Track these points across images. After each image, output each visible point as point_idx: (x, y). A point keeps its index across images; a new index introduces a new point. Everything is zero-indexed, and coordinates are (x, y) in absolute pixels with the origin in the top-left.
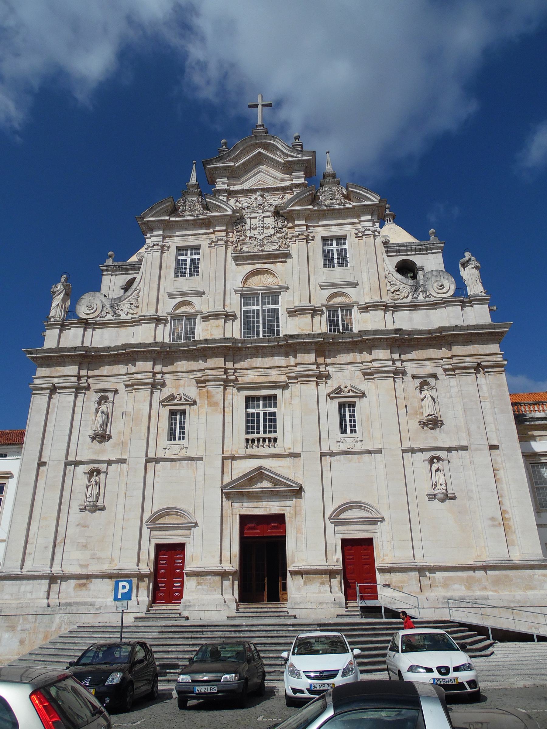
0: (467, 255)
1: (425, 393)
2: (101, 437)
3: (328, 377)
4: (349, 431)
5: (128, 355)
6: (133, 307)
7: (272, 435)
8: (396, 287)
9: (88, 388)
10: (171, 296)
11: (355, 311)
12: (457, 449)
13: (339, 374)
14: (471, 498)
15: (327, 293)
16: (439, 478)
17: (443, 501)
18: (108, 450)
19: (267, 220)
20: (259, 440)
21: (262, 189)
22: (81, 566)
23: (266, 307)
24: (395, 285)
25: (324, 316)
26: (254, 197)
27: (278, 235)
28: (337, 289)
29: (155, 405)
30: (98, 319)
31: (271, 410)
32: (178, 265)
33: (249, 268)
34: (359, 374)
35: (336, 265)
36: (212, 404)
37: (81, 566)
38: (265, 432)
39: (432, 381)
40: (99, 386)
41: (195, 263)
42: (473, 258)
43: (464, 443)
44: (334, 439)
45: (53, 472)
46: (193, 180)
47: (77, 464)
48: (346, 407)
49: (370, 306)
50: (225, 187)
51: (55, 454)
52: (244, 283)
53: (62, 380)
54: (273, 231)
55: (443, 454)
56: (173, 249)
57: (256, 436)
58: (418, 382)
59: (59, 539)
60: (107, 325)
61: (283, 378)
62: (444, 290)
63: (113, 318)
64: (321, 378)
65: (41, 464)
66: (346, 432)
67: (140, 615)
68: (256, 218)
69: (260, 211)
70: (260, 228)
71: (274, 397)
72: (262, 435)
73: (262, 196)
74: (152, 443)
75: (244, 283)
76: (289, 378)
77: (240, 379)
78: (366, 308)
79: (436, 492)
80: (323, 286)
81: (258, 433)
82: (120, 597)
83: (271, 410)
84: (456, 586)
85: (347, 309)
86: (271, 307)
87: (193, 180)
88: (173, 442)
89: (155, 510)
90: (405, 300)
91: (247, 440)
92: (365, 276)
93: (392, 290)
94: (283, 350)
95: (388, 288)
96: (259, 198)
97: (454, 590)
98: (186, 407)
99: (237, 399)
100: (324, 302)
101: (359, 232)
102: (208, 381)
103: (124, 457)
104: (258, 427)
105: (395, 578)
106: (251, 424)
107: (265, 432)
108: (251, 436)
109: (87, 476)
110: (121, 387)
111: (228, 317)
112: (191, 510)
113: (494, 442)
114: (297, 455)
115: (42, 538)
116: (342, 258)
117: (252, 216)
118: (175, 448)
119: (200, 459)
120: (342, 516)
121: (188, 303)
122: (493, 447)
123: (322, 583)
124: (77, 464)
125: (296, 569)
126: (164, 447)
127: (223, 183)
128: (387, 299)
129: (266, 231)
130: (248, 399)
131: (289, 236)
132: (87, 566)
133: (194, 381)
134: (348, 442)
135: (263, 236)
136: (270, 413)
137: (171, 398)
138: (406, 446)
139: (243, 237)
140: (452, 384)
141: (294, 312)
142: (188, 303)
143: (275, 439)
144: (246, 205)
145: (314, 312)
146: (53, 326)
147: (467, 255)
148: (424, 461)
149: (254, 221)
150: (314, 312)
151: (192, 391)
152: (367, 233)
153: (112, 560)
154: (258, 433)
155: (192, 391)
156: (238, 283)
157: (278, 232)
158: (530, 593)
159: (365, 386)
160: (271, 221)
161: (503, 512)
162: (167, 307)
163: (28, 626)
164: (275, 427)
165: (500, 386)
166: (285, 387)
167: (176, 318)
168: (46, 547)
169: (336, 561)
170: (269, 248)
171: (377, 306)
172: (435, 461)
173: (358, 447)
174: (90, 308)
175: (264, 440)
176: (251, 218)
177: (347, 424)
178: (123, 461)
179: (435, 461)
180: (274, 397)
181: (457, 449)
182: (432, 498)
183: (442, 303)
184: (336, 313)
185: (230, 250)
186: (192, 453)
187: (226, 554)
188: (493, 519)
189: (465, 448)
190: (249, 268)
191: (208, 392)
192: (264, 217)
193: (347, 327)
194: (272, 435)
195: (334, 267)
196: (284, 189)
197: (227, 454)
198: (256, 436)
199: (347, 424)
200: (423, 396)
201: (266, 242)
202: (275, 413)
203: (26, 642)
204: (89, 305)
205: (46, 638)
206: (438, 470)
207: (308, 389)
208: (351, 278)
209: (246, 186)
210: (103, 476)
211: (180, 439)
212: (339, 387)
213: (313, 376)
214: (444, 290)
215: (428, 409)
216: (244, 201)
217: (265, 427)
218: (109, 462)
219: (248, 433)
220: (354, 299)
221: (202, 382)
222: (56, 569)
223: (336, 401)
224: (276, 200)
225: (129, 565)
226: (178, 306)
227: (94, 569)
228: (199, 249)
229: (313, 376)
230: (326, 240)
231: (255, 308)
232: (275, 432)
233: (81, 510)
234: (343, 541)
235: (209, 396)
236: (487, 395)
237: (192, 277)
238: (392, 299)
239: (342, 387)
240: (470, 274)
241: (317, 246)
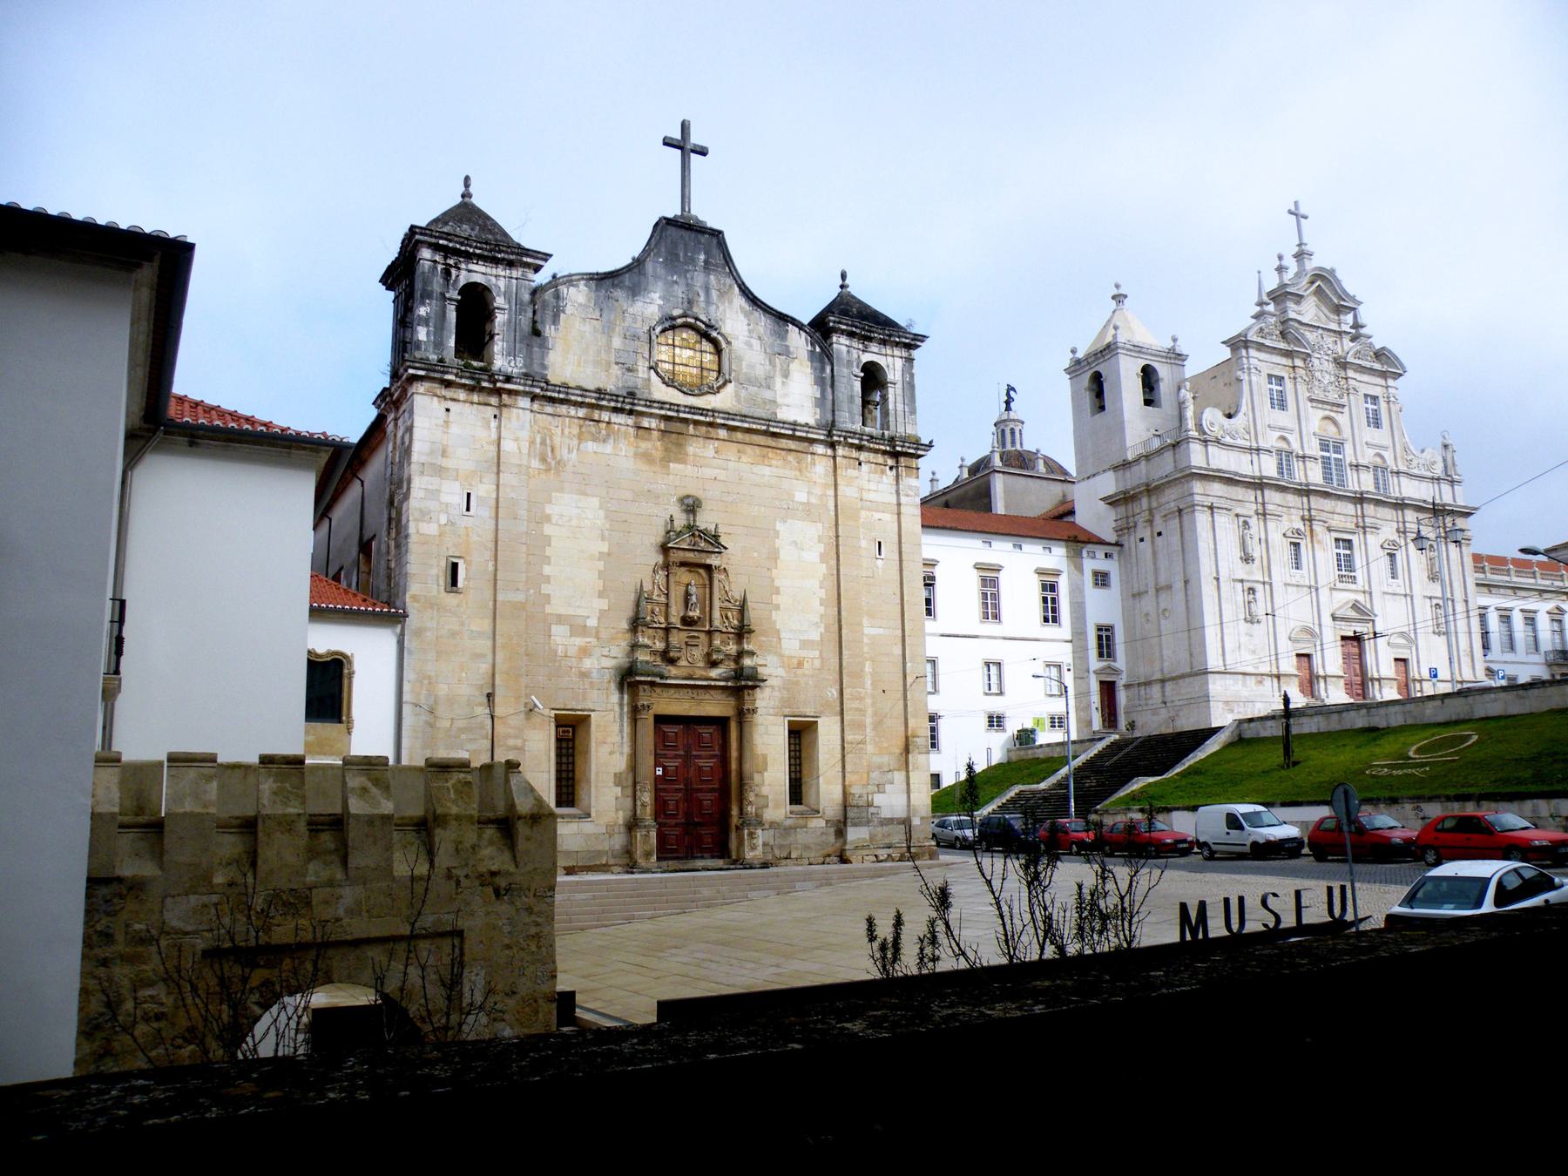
5: (1259, 485)
15: (1372, 452)
33: (1322, 413)
40: (1239, 511)
71: (1349, 541)
99: (1329, 540)
121: (1284, 438)
130: (1337, 540)
160: (1331, 367)
162: (1270, 440)
167: (1279, 452)
170: (1333, 396)
190: (1322, 413)
216: (1311, 336)
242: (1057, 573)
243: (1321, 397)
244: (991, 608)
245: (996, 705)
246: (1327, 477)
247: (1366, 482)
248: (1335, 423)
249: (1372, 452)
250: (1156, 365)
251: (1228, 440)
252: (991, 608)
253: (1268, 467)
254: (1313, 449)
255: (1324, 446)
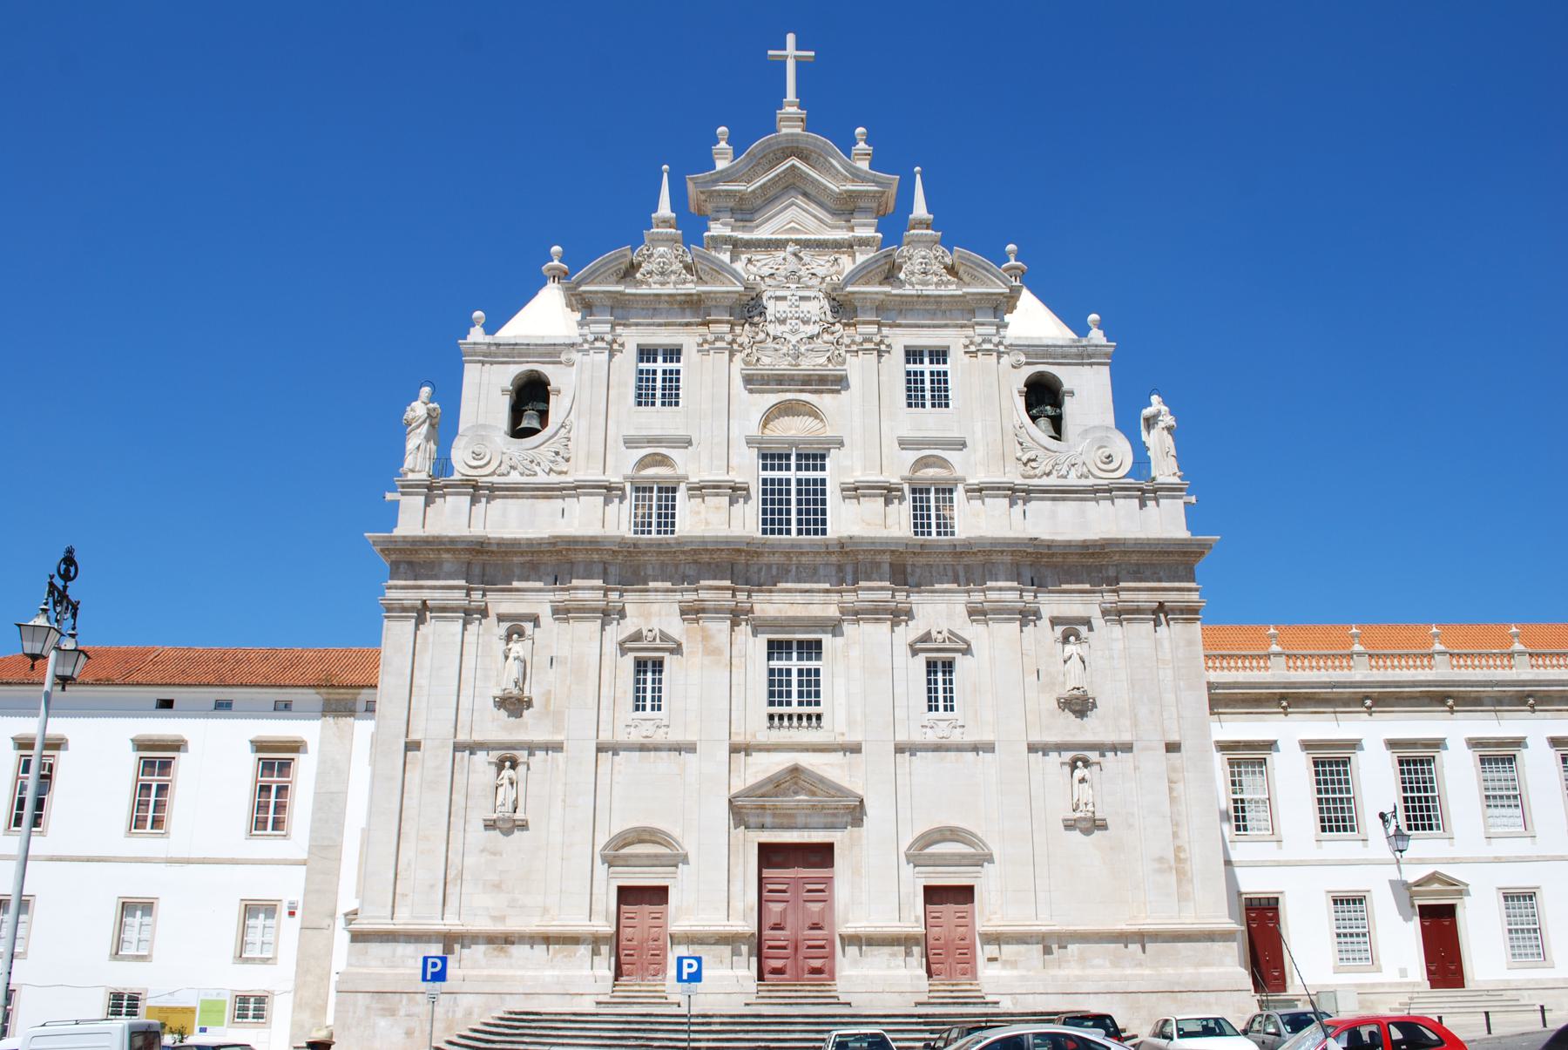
0: (1155, 399)
1: (1071, 649)
2: (514, 704)
3: (909, 614)
4: (941, 708)
6: (559, 459)
7: (813, 710)
8: (1031, 455)
9: (484, 613)
10: (630, 443)
11: (959, 495)
12: (1115, 748)
13: (929, 607)
14: (1130, 826)
15: (912, 456)
16: (1084, 793)
17: (1087, 832)
18: (531, 728)
19: (805, 306)
20: (790, 717)
21: (797, 242)
22: (494, 918)
23: (804, 475)
24: (1030, 449)
25: (906, 504)
26: (782, 254)
27: (826, 337)
28: (929, 451)
29: (611, 648)
30: (495, 479)
31: (812, 664)
32: (641, 380)
33: (773, 399)
34: (961, 610)
35: (928, 403)
36: (712, 652)
37: (494, 918)
38: (800, 704)
39: (1083, 630)
41: (672, 378)
42: (1164, 409)
43: (1126, 737)
44: (918, 724)
45: (435, 757)
46: (665, 209)
47: (473, 748)
48: (940, 669)
49: (987, 489)
50: (727, 232)
51: (434, 727)
52: (764, 426)
53: (438, 594)
54: (815, 329)
55: (1093, 756)
56: (631, 352)
57: (784, 710)
58: (1059, 630)
59: (452, 874)
60: (513, 491)
61: (833, 611)
62: (1111, 466)
63: (525, 479)
64: (900, 616)
65: (412, 746)
66: (937, 709)
67: (602, 998)
68: (784, 298)
69: (793, 286)
70: (796, 315)
72: (795, 709)
73: (795, 255)
74: (605, 715)
75: (764, 426)
76: (842, 613)
77: (757, 607)
78: (979, 491)
79: (1078, 815)
80: (904, 444)
81: (789, 704)
82: (685, 977)
83: (812, 664)
84: (1097, 961)
85: (946, 491)
86: (811, 475)
87: (665, 209)
88: (640, 714)
89: (616, 831)
90: (1045, 481)
91: (771, 717)
92: (978, 427)
93: (1025, 459)
94: (834, 559)
95: (1019, 454)
96: (791, 258)
97: (1093, 967)
98: (666, 655)
100: (906, 473)
101: (972, 343)
102: (704, 610)
103: (558, 738)
104: (789, 694)
105: (1008, 950)
106: (777, 689)
107: (800, 704)
108: (777, 710)
109: (493, 769)
110: (545, 611)
111: (737, 492)
112: (676, 832)
113: (1174, 738)
114: (855, 749)
115: (422, 870)
116: (939, 390)
117: (779, 293)
118: (645, 727)
119: (691, 748)
120: (928, 851)
121: (663, 461)
122: (1172, 747)
123: (894, 955)
124: (473, 748)
125: (851, 931)
126: (626, 724)
127: (725, 224)
128: (1014, 476)
129: (803, 328)
131: (847, 341)
132: (502, 919)
133: (676, 606)
134: (940, 727)
135: (798, 337)
136: (809, 671)
137: (637, 636)
138: (1036, 737)
139: (762, 336)
140: (1114, 636)
141: (854, 491)
142: (663, 461)
143: (819, 717)
144: (766, 271)
145: (889, 493)
146: (409, 488)
147: (1155, 399)
148: (1063, 764)
149: (782, 306)
150: (889, 493)
151: (676, 627)
152: (985, 346)
153: (545, 910)
154: (789, 704)
155: (676, 627)
156: (754, 429)
157: (825, 330)
158: (1205, 970)
159: (973, 632)
161: (1178, 849)
162: (622, 465)
163: (416, 1010)
164: (817, 694)
165: (1190, 643)
166: (835, 628)
168: (432, 886)
169: (912, 918)
170: (813, 363)
171: (999, 489)
172: (1080, 764)
173: (956, 737)
174: (477, 456)
175: (800, 717)
176: (778, 298)
177: (939, 695)
178: (558, 747)
179: (1080, 764)
180: (819, 644)
181: (1115, 748)
182: (1069, 825)
183: (1108, 492)
184: (928, 496)
185: (738, 357)
186: (675, 736)
187: (737, 905)
188: (1161, 860)
189: (1128, 748)
190: (773, 399)
191: (703, 629)
192: (802, 298)
193: (945, 526)
194: (813, 710)
195: (923, 406)
196: (837, 245)
197: (737, 739)
198: (784, 710)
199: (939, 695)
200: (1067, 655)
201: (803, 349)
202: (817, 672)
203: (417, 1034)
204: (477, 450)
205: (448, 1028)
206: (1082, 780)
207: (878, 632)
208: (954, 434)
209: (763, 233)
210: (521, 769)
211: (653, 708)
212: (929, 633)
213: (885, 611)
214: (1111, 466)
215: (1073, 679)
217: (800, 694)
218: (531, 748)
219: (771, 704)
220: (959, 473)
221: (691, 613)
222: (452, 923)
223: (922, 657)
224: (820, 264)
225: (575, 920)
226: (643, 463)
227: (513, 925)
228: (679, 352)
229: (885, 611)
230: (913, 355)
231: (783, 474)
232: (818, 703)
233: (487, 827)
234: (926, 888)
235: (706, 638)
236: (1169, 657)
237: (667, 408)
238: (1025, 477)
239: (934, 634)
240: (1158, 442)
241: (896, 365)
242: (296, 747)
243: (783, 366)
244: (150, 807)
245: (127, 978)
246: (773, 518)
247: (897, 523)
248: (814, 413)
249: (912, 456)
250: (547, 370)
251: (515, 477)
252: (150, 807)
253: (618, 521)
254: (748, 469)
255: (772, 458)
